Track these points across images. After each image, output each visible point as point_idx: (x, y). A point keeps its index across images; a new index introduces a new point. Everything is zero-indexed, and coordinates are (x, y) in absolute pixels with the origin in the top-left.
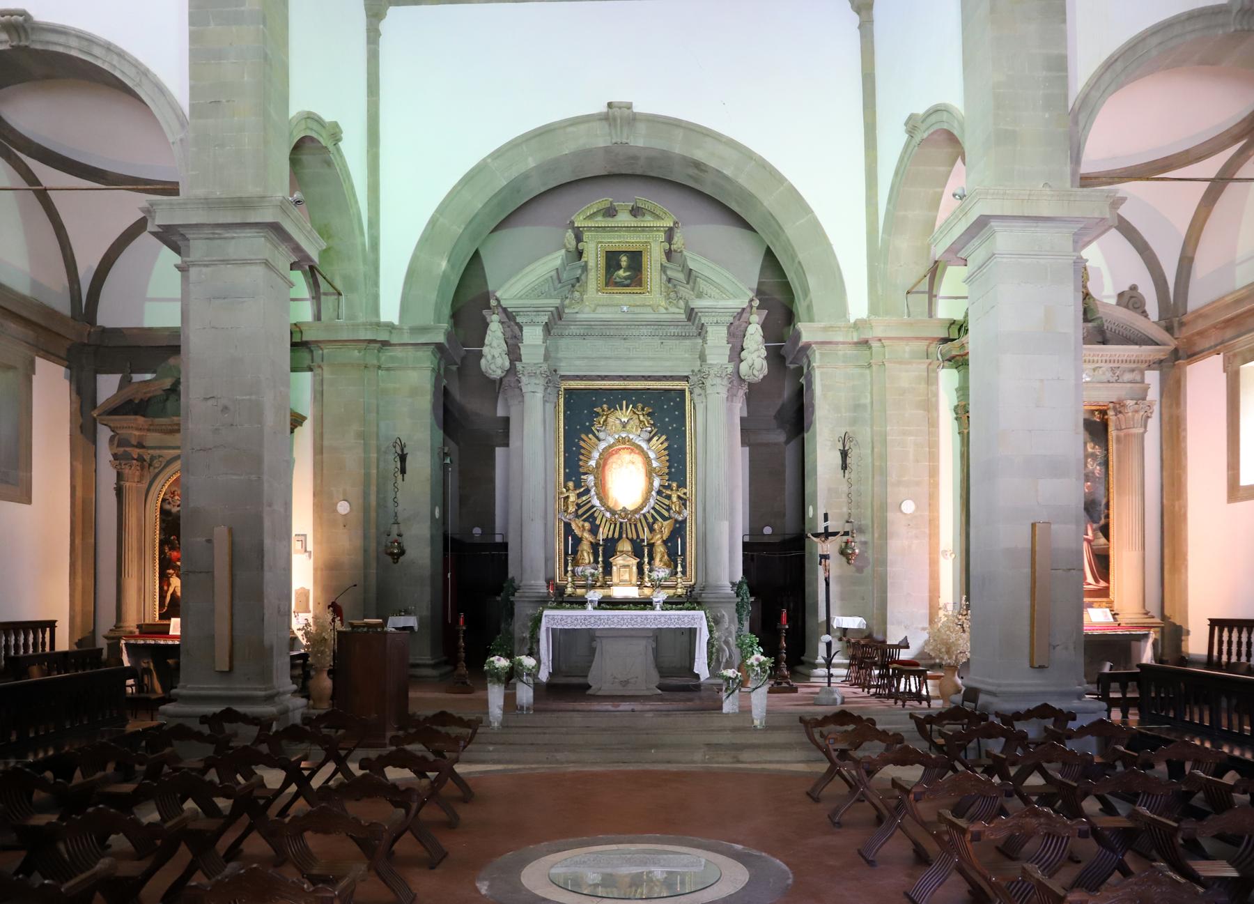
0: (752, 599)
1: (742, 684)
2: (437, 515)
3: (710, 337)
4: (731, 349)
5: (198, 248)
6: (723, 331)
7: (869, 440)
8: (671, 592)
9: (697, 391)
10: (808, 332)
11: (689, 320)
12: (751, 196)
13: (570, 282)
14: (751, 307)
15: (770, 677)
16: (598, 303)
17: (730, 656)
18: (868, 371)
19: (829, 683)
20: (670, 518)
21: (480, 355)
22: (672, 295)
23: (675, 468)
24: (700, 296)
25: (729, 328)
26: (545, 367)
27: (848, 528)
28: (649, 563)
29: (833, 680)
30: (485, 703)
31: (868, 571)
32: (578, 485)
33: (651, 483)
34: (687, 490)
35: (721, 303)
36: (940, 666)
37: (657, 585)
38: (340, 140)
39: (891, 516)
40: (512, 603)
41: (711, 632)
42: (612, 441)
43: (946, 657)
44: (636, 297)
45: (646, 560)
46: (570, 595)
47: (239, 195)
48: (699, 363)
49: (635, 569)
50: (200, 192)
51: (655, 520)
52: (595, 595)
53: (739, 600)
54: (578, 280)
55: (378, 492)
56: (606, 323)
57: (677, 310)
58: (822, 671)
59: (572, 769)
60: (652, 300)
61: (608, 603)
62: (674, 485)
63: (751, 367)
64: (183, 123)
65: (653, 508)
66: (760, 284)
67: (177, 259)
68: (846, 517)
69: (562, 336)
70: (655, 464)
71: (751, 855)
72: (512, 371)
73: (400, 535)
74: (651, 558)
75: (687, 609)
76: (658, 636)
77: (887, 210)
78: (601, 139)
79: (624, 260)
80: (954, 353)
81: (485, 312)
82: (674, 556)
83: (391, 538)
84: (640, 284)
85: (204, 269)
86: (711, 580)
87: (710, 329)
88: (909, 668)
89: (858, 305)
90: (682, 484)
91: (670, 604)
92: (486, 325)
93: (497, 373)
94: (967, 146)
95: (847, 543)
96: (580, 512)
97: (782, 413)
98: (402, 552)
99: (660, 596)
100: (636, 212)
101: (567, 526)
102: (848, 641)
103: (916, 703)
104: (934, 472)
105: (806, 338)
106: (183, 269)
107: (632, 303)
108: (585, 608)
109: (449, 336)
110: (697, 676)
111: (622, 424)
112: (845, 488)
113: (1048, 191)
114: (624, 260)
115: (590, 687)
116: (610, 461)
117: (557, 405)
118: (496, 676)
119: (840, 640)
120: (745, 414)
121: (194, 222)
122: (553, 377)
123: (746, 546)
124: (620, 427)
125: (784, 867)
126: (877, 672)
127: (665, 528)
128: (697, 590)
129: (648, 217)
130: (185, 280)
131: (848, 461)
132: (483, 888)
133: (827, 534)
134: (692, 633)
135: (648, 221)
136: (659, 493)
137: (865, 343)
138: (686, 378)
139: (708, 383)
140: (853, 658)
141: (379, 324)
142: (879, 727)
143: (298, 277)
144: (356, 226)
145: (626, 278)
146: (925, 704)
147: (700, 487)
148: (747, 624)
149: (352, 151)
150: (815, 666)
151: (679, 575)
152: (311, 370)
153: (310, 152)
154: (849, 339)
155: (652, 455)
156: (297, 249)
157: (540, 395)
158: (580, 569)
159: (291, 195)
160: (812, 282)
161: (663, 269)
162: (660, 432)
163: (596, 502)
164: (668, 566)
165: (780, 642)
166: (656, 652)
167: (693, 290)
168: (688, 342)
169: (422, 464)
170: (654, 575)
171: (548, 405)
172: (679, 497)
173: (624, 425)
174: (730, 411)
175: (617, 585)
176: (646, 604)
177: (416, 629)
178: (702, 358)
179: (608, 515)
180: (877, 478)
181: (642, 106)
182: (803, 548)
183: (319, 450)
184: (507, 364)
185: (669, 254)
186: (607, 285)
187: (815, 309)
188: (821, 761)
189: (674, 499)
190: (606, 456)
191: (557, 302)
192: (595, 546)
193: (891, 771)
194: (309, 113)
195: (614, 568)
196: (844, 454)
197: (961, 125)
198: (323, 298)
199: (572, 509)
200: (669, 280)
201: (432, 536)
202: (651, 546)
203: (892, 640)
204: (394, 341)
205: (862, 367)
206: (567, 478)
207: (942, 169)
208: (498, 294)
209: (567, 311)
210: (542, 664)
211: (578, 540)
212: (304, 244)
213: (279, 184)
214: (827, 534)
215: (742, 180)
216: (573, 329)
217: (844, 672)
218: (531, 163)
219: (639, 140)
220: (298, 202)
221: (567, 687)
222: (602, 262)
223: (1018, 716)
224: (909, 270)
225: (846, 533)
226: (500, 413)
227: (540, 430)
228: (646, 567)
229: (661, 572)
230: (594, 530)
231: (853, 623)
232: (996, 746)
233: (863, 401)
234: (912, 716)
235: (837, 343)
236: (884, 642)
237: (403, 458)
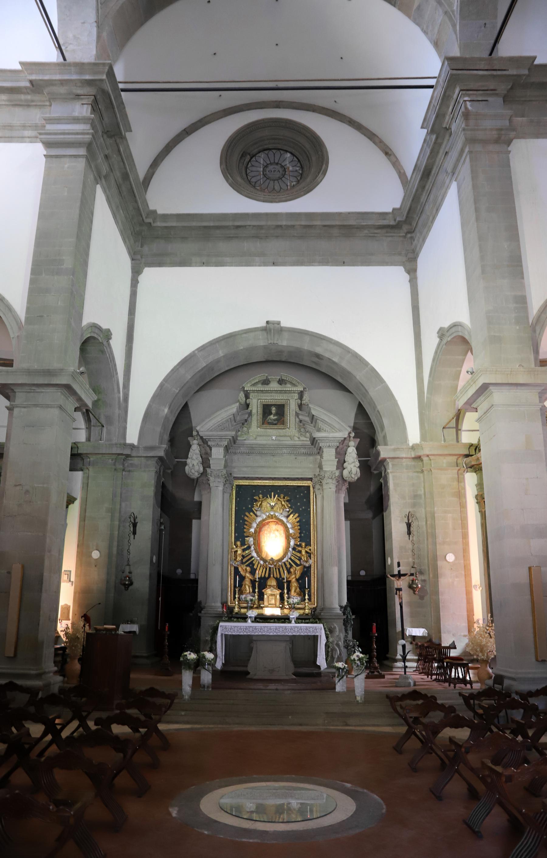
0: (354, 617)
1: (348, 672)
2: (154, 561)
3: (325, 455)
4: (338, 462)
5: (20, 397)
6: (333, 451)
7: (424, 516)
8: (302, 612)
9: (317, 486)
10: (384, 452)
11: (312, 444)
12: (349, 373)
13: (242, 421)
14: (350, 437)
15: (366, 668)
16: (257, 434)
17: (340, 654)
18: (421, 475)
19: (405, 672)
20: (301, 565)
21: (185, 464)
22: (302, 430)
23: (304, 534)
24: (319, 430)
25: (336, 449)
26: (224, 472)
27: (413, 571)
28: (288, 593)
29: (407, 670)
30: (180, 682)
31: (427, 598)
32: (243, 544)
33: (288, 543)
34: (312, 548)
35: (331, 435)
36: (477, 661)
37: (293, 608)
38: (110, 339)
39: (440, 563)
40: (200, 618)
41: (327, 638)
42: (264, 517)
43: (480, 654)
44: (280, 431)
45: (286, 591)
46: (237, 613)
47: (47, 368)
48: (318, 470)
49: (278, 597)
50: (25, 365)
52: (252, 613)
53: (345, 617)
54: (246, 421)
55: (118, 546)
56: (263, 446)
57: (305, 439)
58: (400, 664)
59: (236, 729)
60: (291, 433)
61: (261, 618)
62: (303, 544)
63: (350, 472)
64: (20, 327)
66: (355, 423)
67: (7, 403)
68: (412, 565)
69: (235, 453)
70: (291, 531)
71: (357, 791)
72: (204, 473)
73: (130, 573)
74: (289, 590)
75: (312, 623)
76: (293, 640)
77: (429, 382)
78: (261, 341)
79: (274, 410)
80: (473, 463)
81: (189, 439)
82: (303, 589)
83: (124, 575)
84: (283, 423)
85: (23, 410)
86: (327, 605)
87: (325, 450)
88: (457, 662)
89: (414, 435)
90: (308, 544)
91: (301, 619)
92: (190, 446)
93: (195, 475)
94: (473, 344)
95: (413, 580)
96: (244, 560)
97: (369, 499)
98: (131, 584)
99: (294, 615)
100: (281, 382)
101: (236, 569)
102: (417, 644)
103: (463, 686)
104: (465, 536)
105: (383, 455)
106: (10, 409)
107: (278, 434)
108: (246, 622)
109: (166, 452)
110: (319, 667)
111: (272, 506)
112: (410, 546)
113: (522, 369)
114: (274, 410)
115: (248, 673)
116: (263, 529)
117: (231, 494)
118: (188, 665)
119: (411, 643)
120: (347, 501)
121: (20, 382)
122: (229, 478)
123: (348, 582)
124: (269, 508)
125: (380, 800)
126: (436, 665)
127: (298, 571)
128: (318, 611)
129: (288, 385)
130: (11, 415)
131: (412, 529)
132: (174, 812)
133: (400, 575)
134: (315, 639)
135: (289, 387)
136: (294, 549)
137: (419, 458)
138: (311, 479)
139: (324, 482)
140: (420, 655)
141: (125, 445)
142: (439, 702)
143: (79, 416)
144: (116, 387)
145: (274, 420)
146: (469, 686)
147: (319, 546)
148: (350, 633)
149: (117, 345)
150: (396, 661)
151: (307, 601)
152: (82, 470)
153: (93, 346)
154: (409, 456)
155: (289, 526)
156: (80, 399)
157: (221, 488)
158: (243, 596)
159: (79, 369)
160: (386, 422)
161: (297, 415)
162: (294, 512)
163: (254, 554)
164: (299, 595)
165: (372, 645)
166: (292, 650)
167: (315, 427)
168: (311, 458)
169: (146, 529)
170: (291, 601)
171: (225, 494)
173: (272, 507)
174: (337, 499)
175: (267, 607)
176: (285, 619)
177: (137, 632)
178: (320, 467)
179: (262, 562)
180: (430, 540)
181: (285, 323)
182: (385, 584)
183: (83, 518)
184: (201, 469)
185: (300, 406)
186: (263, 424)
187: (388, 438)
188: (402, 725)
189: (303, 553)
190: (261, 526)
191: (233, 433)
192: (253, 582)
193: (448, 732)
194: (94, 324)
195: (265, 596)
196: (409, 525)
197: (469, 333)
198: (92, 428)
199: (239, 558)
200: (301, 421)
201: (150, 575)
202: (289, 582)
203: (445, 643)
204: (134, 454)
205: (418, 472)
206: (236, 539)
207: (461, 357)
208: (198, 428)
209: (239, 438)
210: (217, 657)
211: (242, 578)
212: (83, 396)
213: (71, 363)
214: (400, 575)
215: (344, 364)
216: (242, 449)
217: (415, 664)
218: (221, 354)
219: (284, 342)
220: (82, 373)
221: (234, 673)
222: (260, 410)
223: (531, 694)
224: (444, 415)
225: (412, 575)
226: (196, 499)
227: (220, 509)
228: (286, 596)
229: (295, 599)
230: (253, 572)
231: (419, 632)
232: (518, 715)
233: (419, 493)
234: (460, 694)
235: (402, 458)
236: (440, 645)
237: (135, 525)
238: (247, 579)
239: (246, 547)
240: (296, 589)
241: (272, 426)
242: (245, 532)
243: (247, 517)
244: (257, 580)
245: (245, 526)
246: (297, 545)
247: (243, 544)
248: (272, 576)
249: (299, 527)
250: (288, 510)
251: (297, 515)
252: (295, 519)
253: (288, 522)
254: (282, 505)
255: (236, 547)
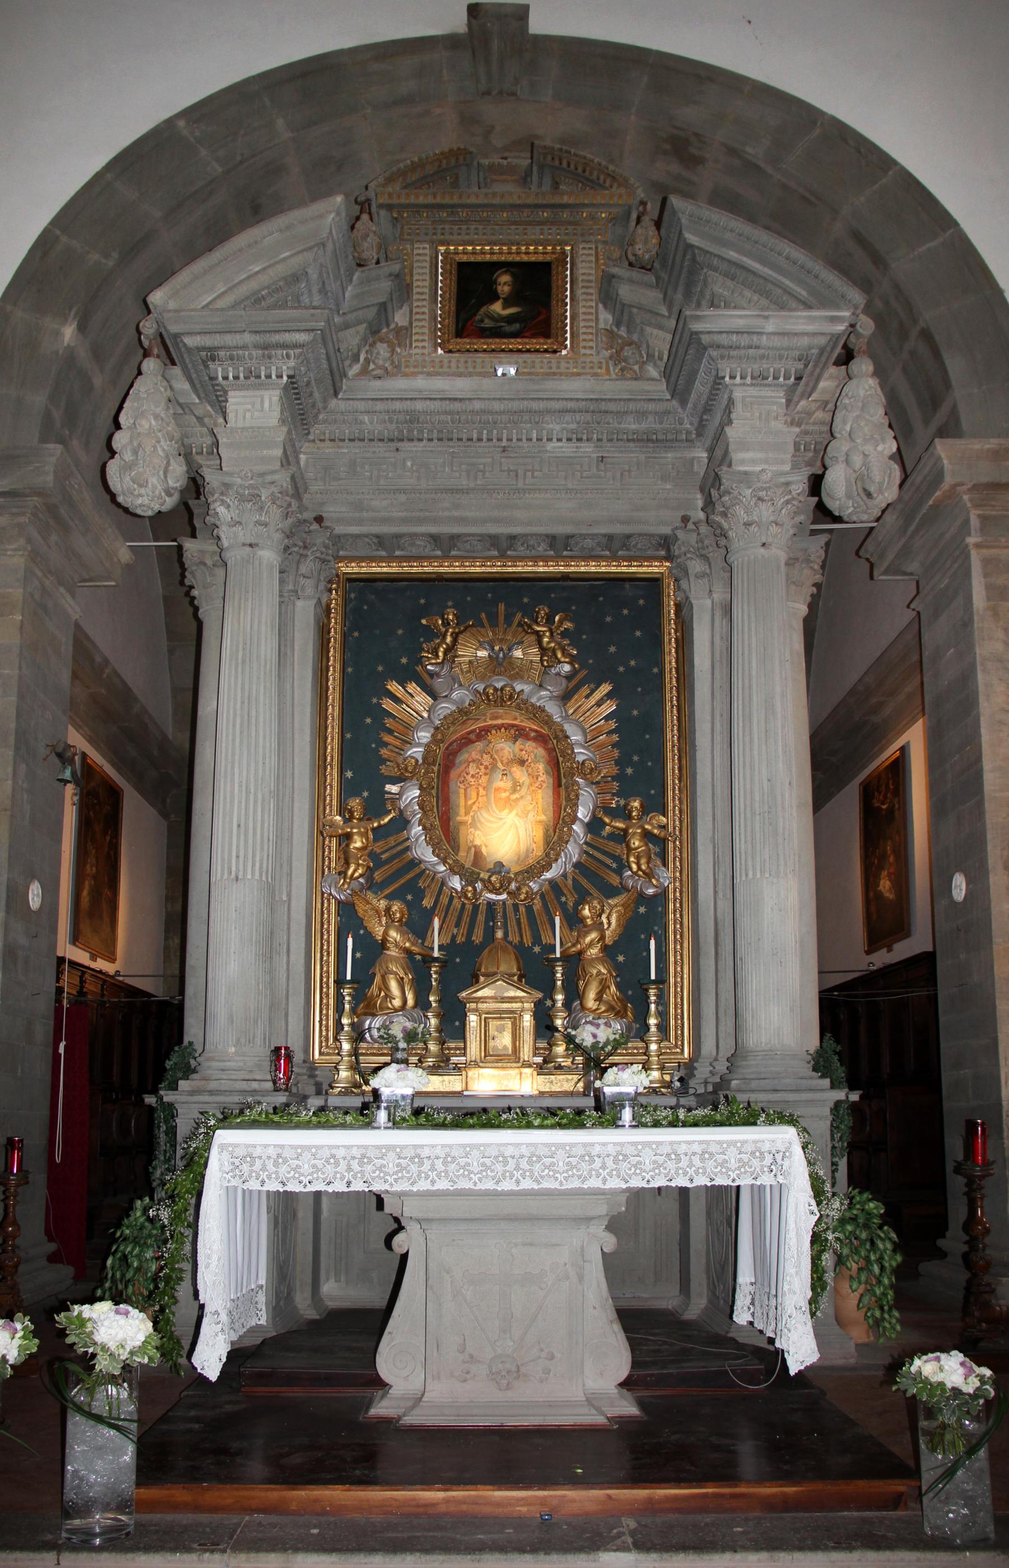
28: (567, 1005)
45: (560, 997)
51: (583, 897)
65: (577, 865)
70: (581, 754)
74: (574, 995)
79: (504, 283)
82: (636, 993)
90: (656, 804)
114: (504, 283)
136: (594, 826)
138: (665, 546)
145: (510, 319)
172: (647, 835)
186: (459, 334)
189: (636, 843)
202: (574, 962)
238: (393, 952)
239: (386, 820)
240: (603, 989)
241: (495, 343)
242: (384, 761)
243: (397, 700)
244: (436, 954)
245: (387, 738)
246: (608, 811)
247: (376, 805)
248: (499, 934)
249: (615, 737)
250: (567, 668)
251: (605, 688)
252: (599, 704)
253: (566, 717)
254: (543, 650)
255: (347, 821)
